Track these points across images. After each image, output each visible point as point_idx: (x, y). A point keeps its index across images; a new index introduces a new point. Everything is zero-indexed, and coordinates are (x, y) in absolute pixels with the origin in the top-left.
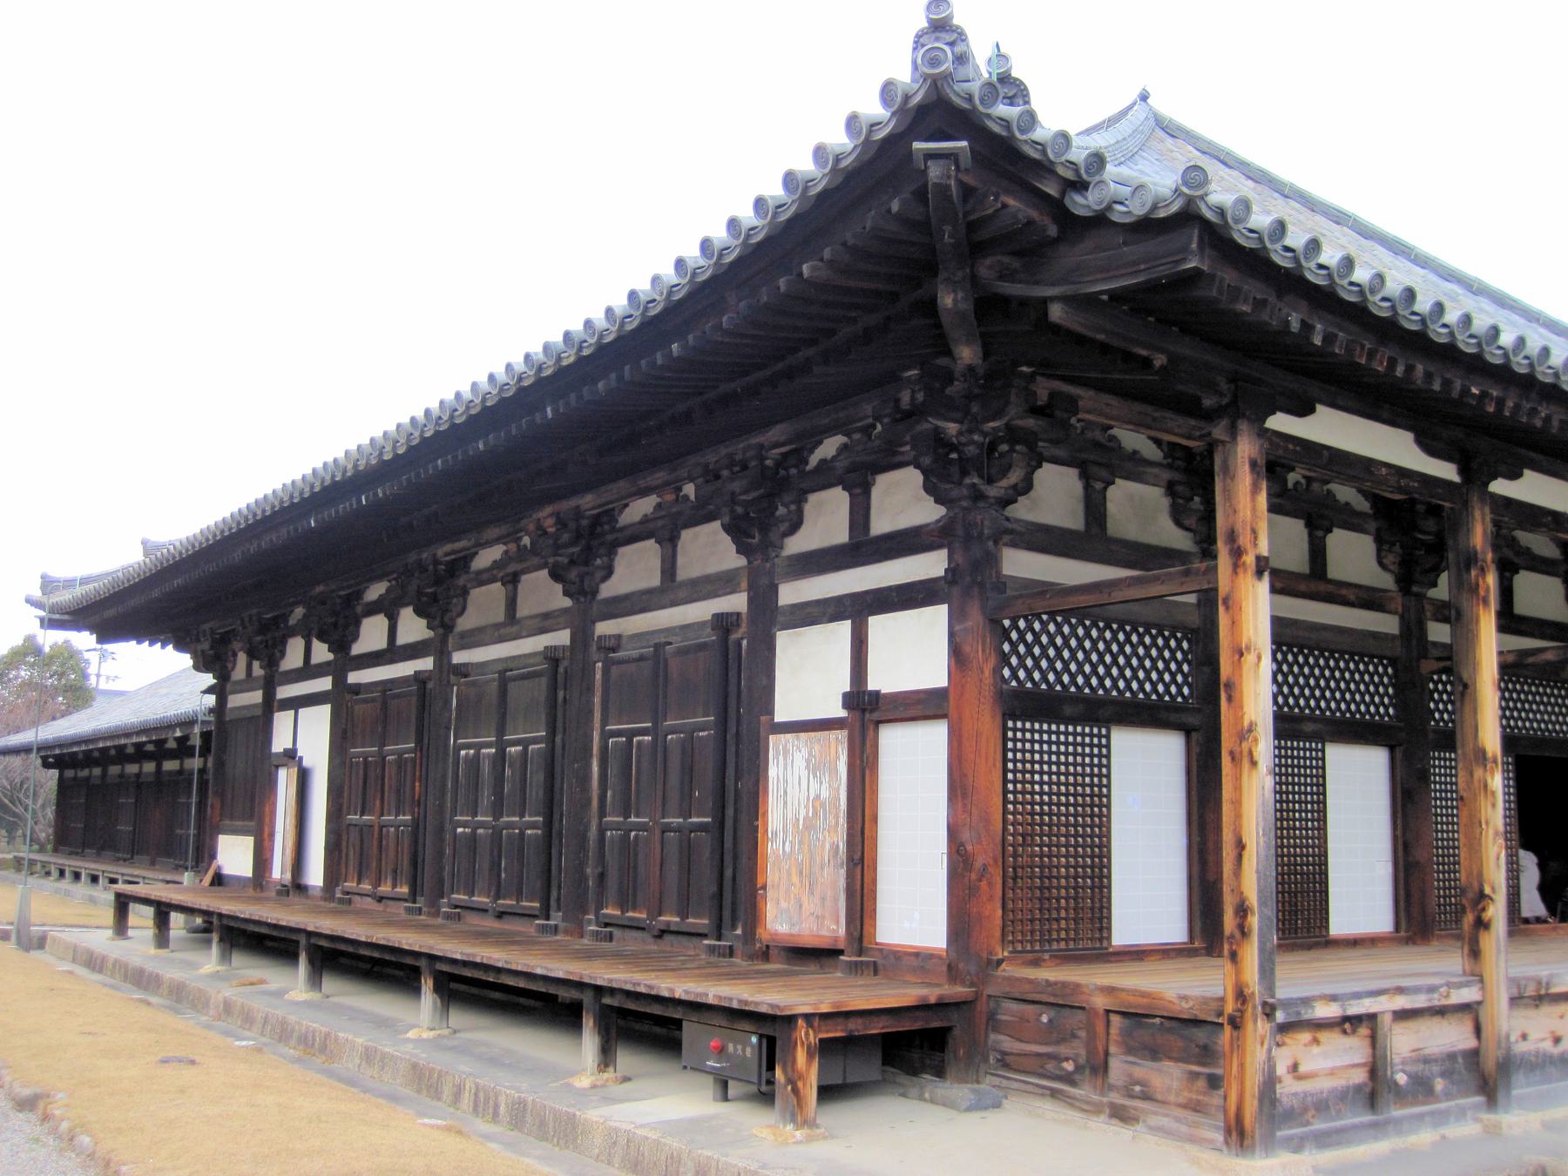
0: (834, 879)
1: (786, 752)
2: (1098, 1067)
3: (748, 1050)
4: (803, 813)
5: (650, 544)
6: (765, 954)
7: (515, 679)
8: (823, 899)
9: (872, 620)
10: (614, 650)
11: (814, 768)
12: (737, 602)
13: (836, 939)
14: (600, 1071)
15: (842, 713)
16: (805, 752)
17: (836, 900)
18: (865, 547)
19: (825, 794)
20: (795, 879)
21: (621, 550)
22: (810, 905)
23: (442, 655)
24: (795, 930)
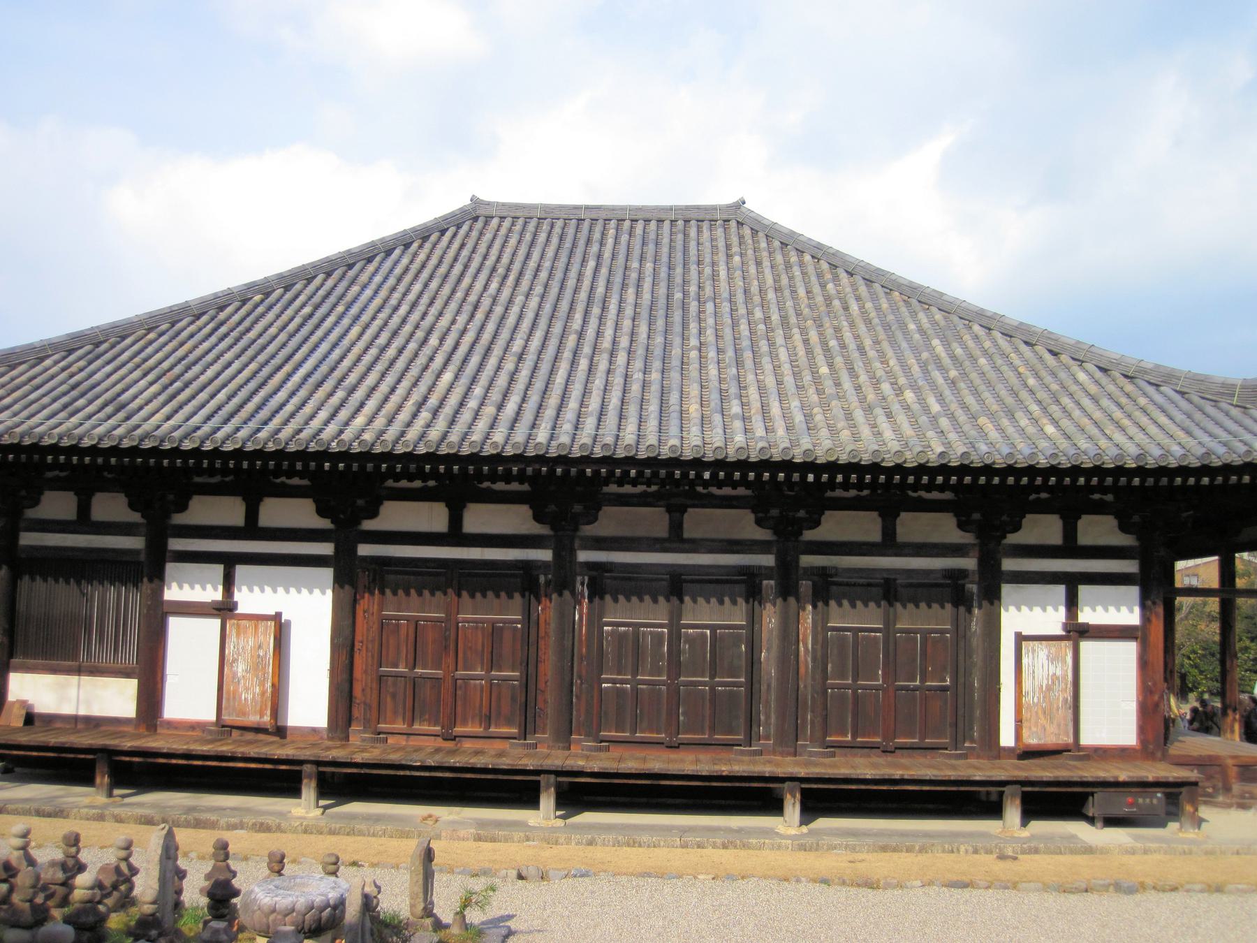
0: (1066, 715)
1: (1034, 651)
2: (1227, 789)
3: (1155, 801)
4: (1045, 682)
5: (875, 514)
6: (998, 757)
7: (692, 581)
8: (1059, 725)
9: (1080, 587)
10: (831, 576)
11: (1052, 659)
12: (969, 563)
13: (1067, 745)
14: (271, 855)
15: (1059, 631)
16: (1046, 651)
17: (1066, 725)
18: (1070, 549)
19: (1059, 673)
20: (1041, 716)
21: (827, 513)
22: (1051, 729)
23: (564, 552)
24: (1042, 742)
